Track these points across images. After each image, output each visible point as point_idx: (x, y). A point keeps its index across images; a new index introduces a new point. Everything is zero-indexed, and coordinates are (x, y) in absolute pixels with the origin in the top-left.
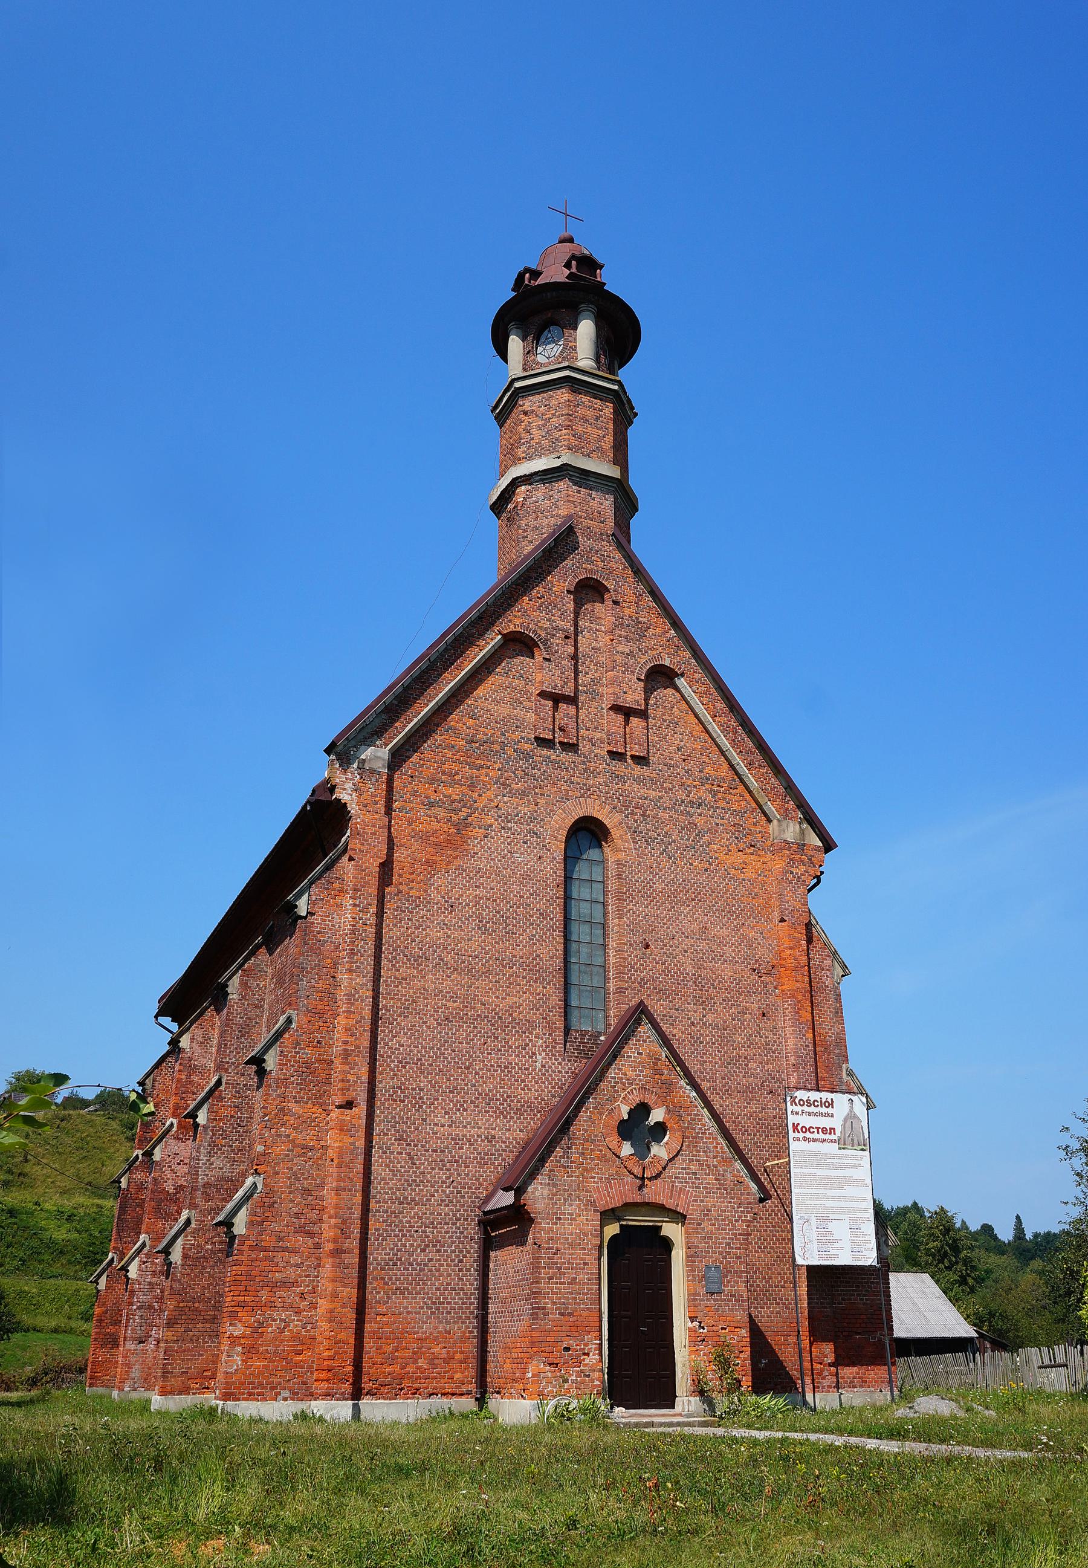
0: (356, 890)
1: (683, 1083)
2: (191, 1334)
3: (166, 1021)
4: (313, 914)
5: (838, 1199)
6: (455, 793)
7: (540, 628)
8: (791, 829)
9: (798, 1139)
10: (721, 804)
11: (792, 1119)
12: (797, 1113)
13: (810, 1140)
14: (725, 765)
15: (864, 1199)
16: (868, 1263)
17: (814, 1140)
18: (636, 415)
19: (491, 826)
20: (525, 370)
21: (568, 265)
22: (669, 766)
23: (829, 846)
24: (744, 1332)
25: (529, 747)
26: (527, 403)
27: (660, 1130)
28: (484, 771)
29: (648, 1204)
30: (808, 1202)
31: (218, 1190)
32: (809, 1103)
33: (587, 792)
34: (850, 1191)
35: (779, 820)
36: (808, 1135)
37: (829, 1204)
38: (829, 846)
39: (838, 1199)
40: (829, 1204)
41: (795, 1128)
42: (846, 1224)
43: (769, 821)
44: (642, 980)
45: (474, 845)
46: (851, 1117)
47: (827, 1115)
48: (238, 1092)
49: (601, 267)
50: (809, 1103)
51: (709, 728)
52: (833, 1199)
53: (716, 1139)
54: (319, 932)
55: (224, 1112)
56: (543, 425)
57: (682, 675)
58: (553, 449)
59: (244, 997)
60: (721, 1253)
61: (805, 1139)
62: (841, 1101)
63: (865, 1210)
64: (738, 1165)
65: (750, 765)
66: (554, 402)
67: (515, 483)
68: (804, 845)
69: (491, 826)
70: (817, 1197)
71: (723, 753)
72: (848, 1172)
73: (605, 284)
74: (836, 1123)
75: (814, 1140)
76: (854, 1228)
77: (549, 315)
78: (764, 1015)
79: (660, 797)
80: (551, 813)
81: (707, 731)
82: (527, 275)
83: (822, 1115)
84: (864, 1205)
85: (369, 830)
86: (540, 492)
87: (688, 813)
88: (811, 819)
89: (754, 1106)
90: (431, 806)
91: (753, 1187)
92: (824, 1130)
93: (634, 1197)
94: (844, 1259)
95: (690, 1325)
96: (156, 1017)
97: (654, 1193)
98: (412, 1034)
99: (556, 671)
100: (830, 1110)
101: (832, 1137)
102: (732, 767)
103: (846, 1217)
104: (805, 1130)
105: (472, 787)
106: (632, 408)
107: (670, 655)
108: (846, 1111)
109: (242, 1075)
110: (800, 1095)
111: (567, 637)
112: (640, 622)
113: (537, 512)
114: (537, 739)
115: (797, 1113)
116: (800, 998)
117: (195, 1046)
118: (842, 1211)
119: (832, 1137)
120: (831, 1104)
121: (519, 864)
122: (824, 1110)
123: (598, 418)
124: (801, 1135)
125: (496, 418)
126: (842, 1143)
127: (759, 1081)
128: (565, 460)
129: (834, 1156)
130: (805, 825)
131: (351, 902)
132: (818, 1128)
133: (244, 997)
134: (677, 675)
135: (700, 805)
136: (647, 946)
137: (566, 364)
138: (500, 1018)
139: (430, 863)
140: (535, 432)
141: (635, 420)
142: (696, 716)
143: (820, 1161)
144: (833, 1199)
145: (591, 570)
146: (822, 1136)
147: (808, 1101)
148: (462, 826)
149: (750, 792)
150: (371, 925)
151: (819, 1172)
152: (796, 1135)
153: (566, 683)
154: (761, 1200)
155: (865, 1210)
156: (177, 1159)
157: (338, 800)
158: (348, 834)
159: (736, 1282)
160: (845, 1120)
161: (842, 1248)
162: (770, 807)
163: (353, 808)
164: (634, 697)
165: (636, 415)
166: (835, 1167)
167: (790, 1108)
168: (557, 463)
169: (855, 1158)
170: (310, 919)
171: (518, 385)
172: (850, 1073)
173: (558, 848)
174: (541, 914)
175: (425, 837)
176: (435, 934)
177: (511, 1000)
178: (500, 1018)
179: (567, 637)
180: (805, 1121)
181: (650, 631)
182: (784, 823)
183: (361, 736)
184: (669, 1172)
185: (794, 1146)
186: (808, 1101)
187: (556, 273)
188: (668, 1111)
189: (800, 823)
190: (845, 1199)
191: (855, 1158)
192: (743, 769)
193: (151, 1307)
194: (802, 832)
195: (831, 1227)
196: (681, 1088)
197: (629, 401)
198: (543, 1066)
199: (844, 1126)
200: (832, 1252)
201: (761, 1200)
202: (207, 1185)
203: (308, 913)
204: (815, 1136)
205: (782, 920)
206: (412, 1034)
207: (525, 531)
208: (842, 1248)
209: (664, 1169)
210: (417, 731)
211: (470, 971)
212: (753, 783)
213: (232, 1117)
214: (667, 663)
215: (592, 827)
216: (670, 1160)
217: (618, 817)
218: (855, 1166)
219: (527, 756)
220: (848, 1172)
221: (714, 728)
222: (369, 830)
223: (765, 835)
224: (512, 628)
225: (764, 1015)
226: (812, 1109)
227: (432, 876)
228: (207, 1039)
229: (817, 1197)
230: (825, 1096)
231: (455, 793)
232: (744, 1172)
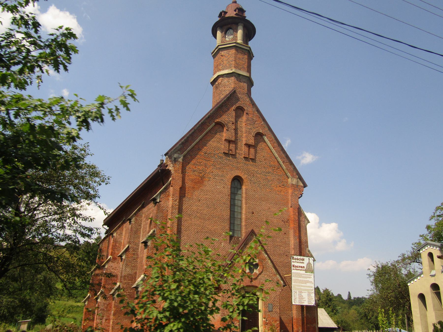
0: (173, 195)
1: (263, 253)
2: (120, 318)
3: (106, 227)
4: (161, 201)
5: (305, 286)
6: (201, 168)
7: (226, 120)
8: (295, 181)
9: (294, 269)
10: (275, 173)
11: (293, 264)
12: (294, 262)
13: (297, 270)
14: (276, 162)
15: (312, 287)
16: (313, 305)
17: (298, 270)
18: (254, 56)
19: (210, 178)
20: (222, 42)
21: (235, 11)
22: (261, 162)
23: (305, 186)
24: (278, 322)
25: (221, 155)
26: (223, 53)
27: (256, 266)
28: (209, 162)
29: (253, 286)
31: (128, 277)
32: (297, 259)
33: (238, 168)
34: (308, 284)
35: (291, 178)
36: (297, 268)
37: (302, 288)
38: (305, 186)
39: (305, 286)
40: (302, 288)
41: (293, 266)
42: (307, 294)
43: (288, 178)
44: (252, 223)
45: (206, 183)
46: (309, 264)
47: (302, 263)
48: (134, 250)
49: (245, 11)
50: (297, 259)
51: (272, 151)
52: (303, 286)
53: (272, 268)
54: (162, 207)
55: (130, 256)
56: (227, 60)
57: (265, 135)
58: (230, 67)
59: (136, 223)
60: (272, 300)
61: (296, 269)
62: (306, 259)
63: (312, 290)
64: (278, 276)
65: (283, 162)
66: (230, 53)
67: (218, 77)
68: (298, 185)
69: (210, 178)
70: (299, 286)
71: (276, 158)
72: (308, 279)
73: (246, 17)
74: (305, 265)
75: (298, 270)
76: (309, 295)
77: (230, 26)
78: (285, 234)
79: (258, 171)
80: (227, 174)
81: (272, 152)
82: (223, 13)
83: (301, 263)
84: (312, 288)
85: (177, 178)
86: (226, 80)
87: (266, 175)
88: (300, 178)
89: (282, 259)
90: (194, 171)
91: (282, 282)
92: (301, 267)
93: (249, 284)
94: (306, 303)
95: (263, 319)
96: (103, 225)
97: (254, 283)
98: (188, 236)
99: (230, 133)
100: (303, 261)
101: (304, 269)
102: (278, 162)
104: (296, 267)
105: (206, 167)
106: (253, 55)
107: (262, 129)
108: (308, 261)
109: (135, 245)
110: (295, 257)
111: (233, 123)
112: (253, 120)
113: (225, 86)
114: (224, 153)
115: (294, 262)
116: (296, 229)
117: (118, 235)
118: (305, 290)
119: (304, 269)
120: (303, 260)
121: (218, 189)
122: (301, 261)
123: (243, 58)
124: (295, 268)
125: (213, 56)
126: (306, 271)
127: (283, 252)
128: (233, 71)
130: (298, 180)
131: (172, 198)
132: (300, 266)
133: (136, 223)
134: (264, 135)
135: (269, 173)
136: (253, 213)
137: (235, 42)
138: (212, 232)
139: (193, 188)
140: (225, 62)
141: (253, 58)
142: (269, 147)
143: (300, 275)
144: (303, 286)
145: (240, 104)
146: (300, 269)
147: (297, 258)
148: (202, 178)
149: (283, 170)
150: (177, 205)
151: (300, 279)
152: (294, 268)
153: (232, 137)
154: (284, 286)
155: (312, 290)
156: (112, 268)
157: (168, 169)
158: (171, 179)
159: (277, 308)
160: (307, 264)
161: (305, 300)
162: (289, 174)
163: (173, 172)
165: (254, 56)
166: (304, 277)
167: (292, 260)
168: (231, 72)
169: (310, 275)
170: (160, 203)
171: (220, 47)
172: (309, 251)
173: (229, 184)
174: (224, 203)
175: (192, 180)
176: (195, 208)
177: (215, 227)
178: (212, 232)
179: (233, 123)
180: (296, 264)
181: (256, 123)
182: (293, 179)
183: (175, 151)
184: (259, 277)
185: (293, 271)
186: (297, 258)
187: (231, 13)
188: (259, 260)
189: (297, 179)
190: (307, 286)
191: (310, 275)
192: (281, 163)
193: (104, 310)
194: (298, 181)
195: (303, 294)
196: (263, 254)
197: (252, 53)
198: (224, 246)
199: (307, 266)
200: (303, 301)
201: (284, 286)
202: (125, 276)
203: (160, 201)
204: (299, 268)
205: (291, 207)
206: (188, 236)
207: (221, 91)
208: (305, 300)
209: (258, 276)
210: (191, 150)
211: (204, 219)
212: (284, 167)
213: (132, 257)
214: (261, 132)
215: (238, 178)
217: (246, 176)
218: (310, 278)
219: (221, 158)
220: (308, 279)
221: (274, 151)
222: (177, 178)
223: (287, 182)
225: (285, 234)
226: (298, 261)
227: (194, 192)
228: (121, 233)
229: (299, 286)
230: (302, 257)
231: (201, 168)
232: (279, 278)
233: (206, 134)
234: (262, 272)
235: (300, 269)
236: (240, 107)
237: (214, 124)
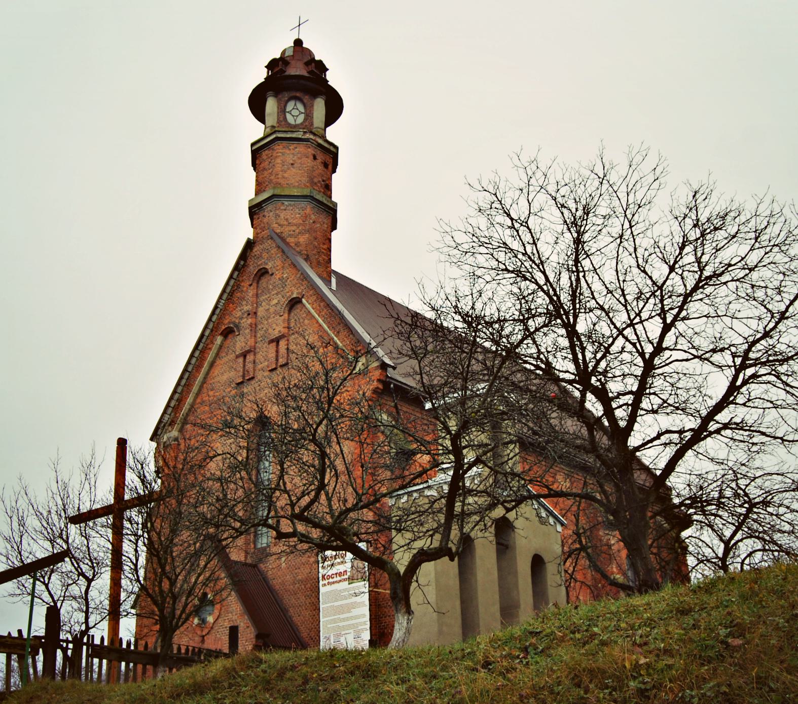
5: (347, 619)
17: (333, 583)
30: (329, 626)
36: (331, 580)
37: (341, 624)
40: (341, 624)
52: (344, 620)
63: (365, 623)
75: (333, 583)
92: (340, 574)
103: (351, 631)
114: (238, 384)
129: (345, 590)
132: (336, 574)
144: (344, 620)
146: (339, 578)
151: (336, 604)
155: (365, 623)
164: (278, 328)
179: (249, 314)
204: (335, 579)
214: (295, 296)
216: (214, 622)
224: (223, 328)
233: (212, 365)
234: (219, 616)
235: (339, 578)
236: (263, 271)
237: (219, 339)
